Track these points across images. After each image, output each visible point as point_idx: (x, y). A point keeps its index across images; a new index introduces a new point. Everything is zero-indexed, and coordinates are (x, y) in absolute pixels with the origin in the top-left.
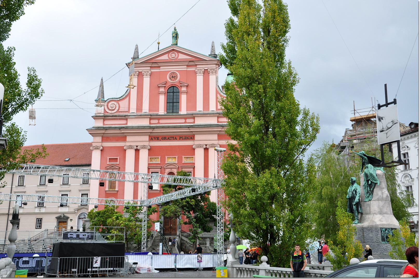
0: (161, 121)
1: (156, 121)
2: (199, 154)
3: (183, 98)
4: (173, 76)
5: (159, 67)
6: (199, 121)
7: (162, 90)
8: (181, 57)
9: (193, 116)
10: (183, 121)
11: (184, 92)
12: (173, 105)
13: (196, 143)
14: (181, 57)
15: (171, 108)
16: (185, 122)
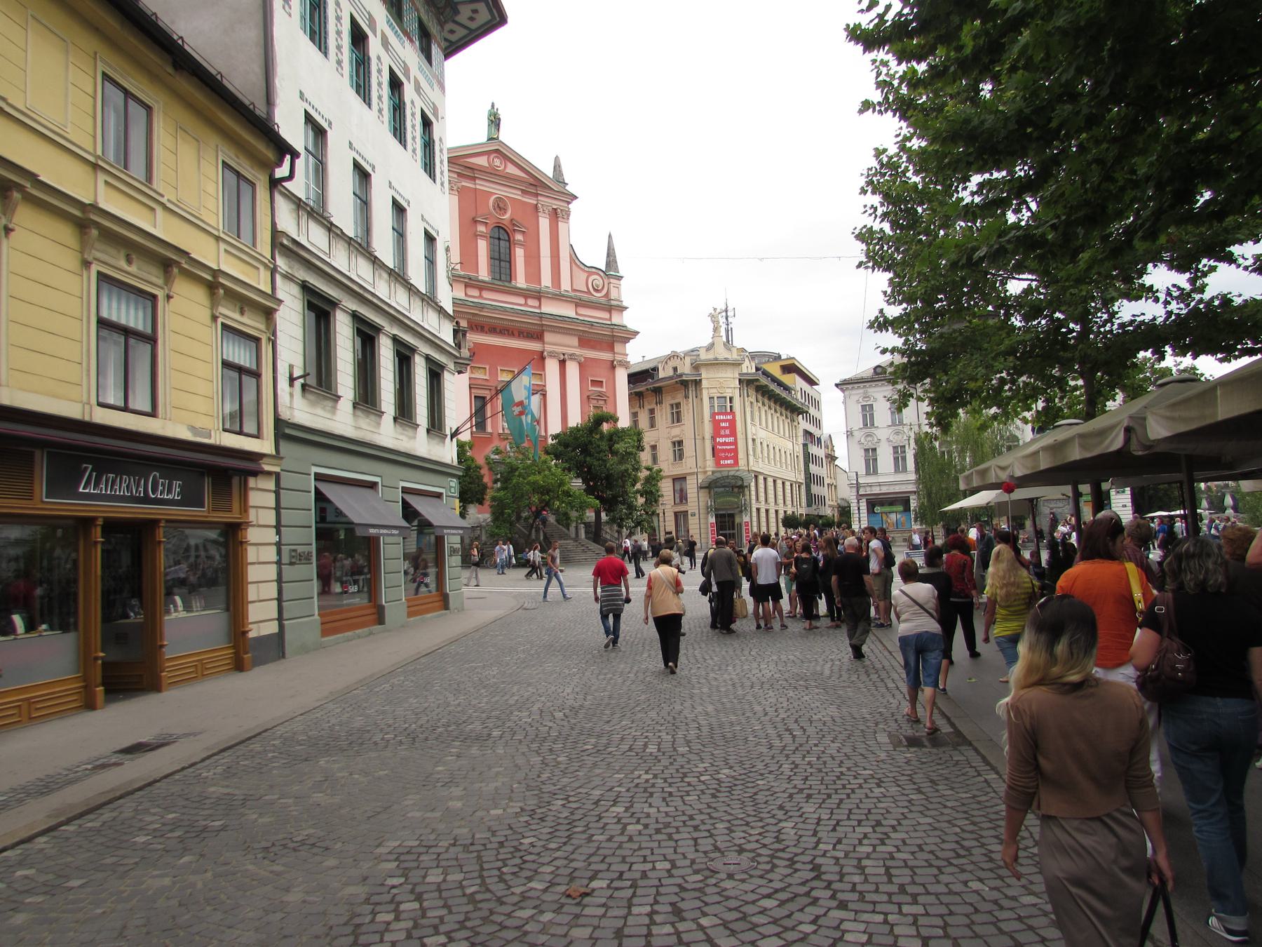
0: (486, 294)
1: (475, 293)
2: (552, 367)
3: (519, 253)
4: (500, 206)
5: (474, 179)
6: (549, 308)
7: (481, 228)
8: (511, 170)
9: (539, 296)
10: (522, 301)
11: (521, 245)
12: (502, 263)
13: (548, 348)
14: (511, 170)
15: (497, 269)
16: (526, 304)
